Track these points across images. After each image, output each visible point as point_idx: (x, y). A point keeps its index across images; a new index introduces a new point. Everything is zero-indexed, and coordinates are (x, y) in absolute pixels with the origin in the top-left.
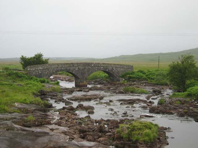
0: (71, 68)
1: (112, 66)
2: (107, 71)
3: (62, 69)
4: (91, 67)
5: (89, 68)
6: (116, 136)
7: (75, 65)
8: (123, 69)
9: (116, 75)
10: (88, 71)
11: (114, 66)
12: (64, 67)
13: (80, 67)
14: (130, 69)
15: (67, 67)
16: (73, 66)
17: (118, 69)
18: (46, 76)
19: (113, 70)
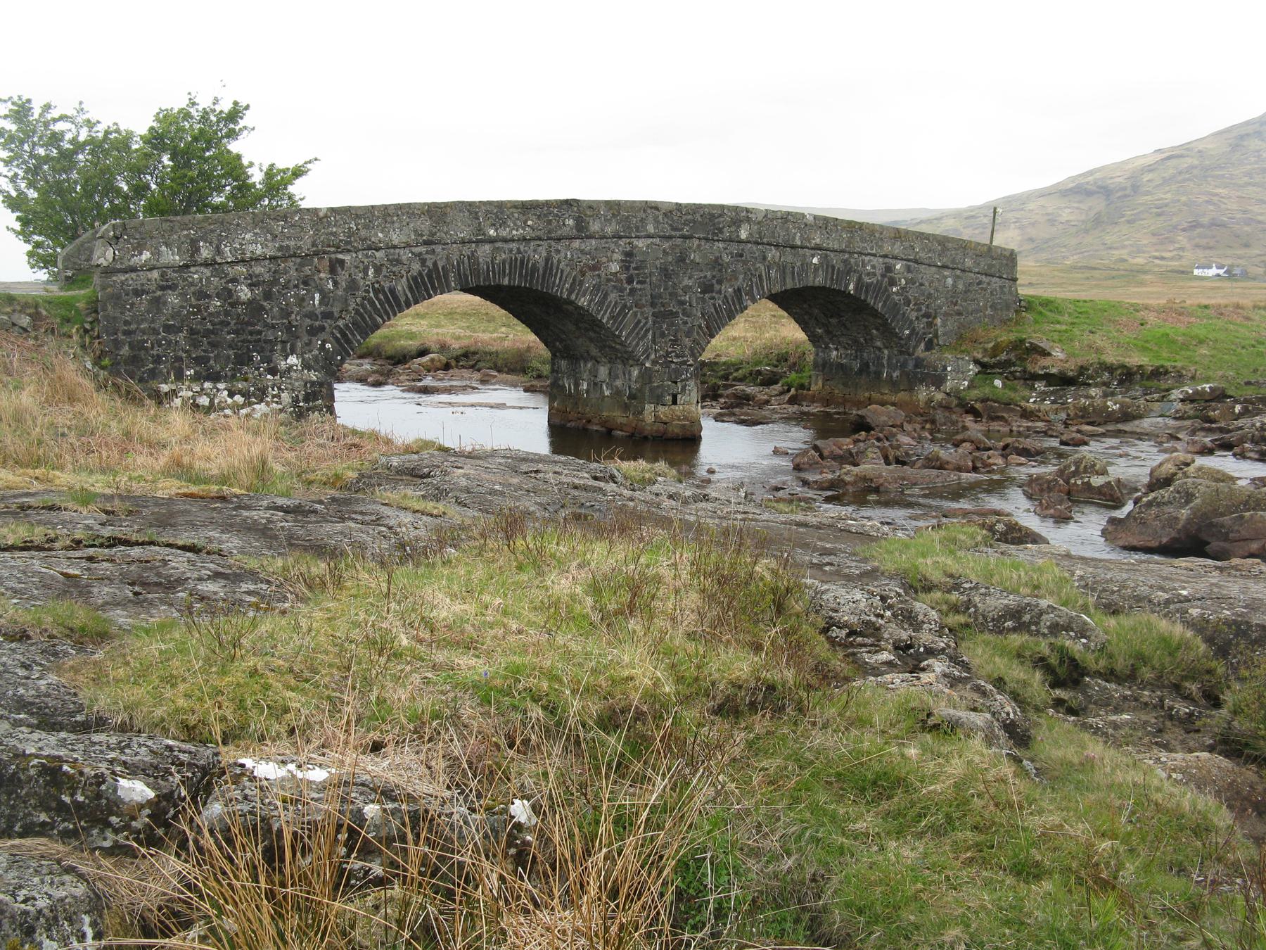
0: (566, 254)
1: (887, 248)
2: (851, 287)
3: (472, 256)
4: (734, 248)
5: (717, 263)
6: (708, 630)
7: (595, 227)
8: (956, 278)
9: (913, 331)
10: (707, 288)
11: (897, 249)
12: (492, 241)
13: (641, 244)
14: (1000, 277)
15: (523, 239)
16: (581, 230)
17: (927, 274)
18: (313, 332)
19: (893, 282)
